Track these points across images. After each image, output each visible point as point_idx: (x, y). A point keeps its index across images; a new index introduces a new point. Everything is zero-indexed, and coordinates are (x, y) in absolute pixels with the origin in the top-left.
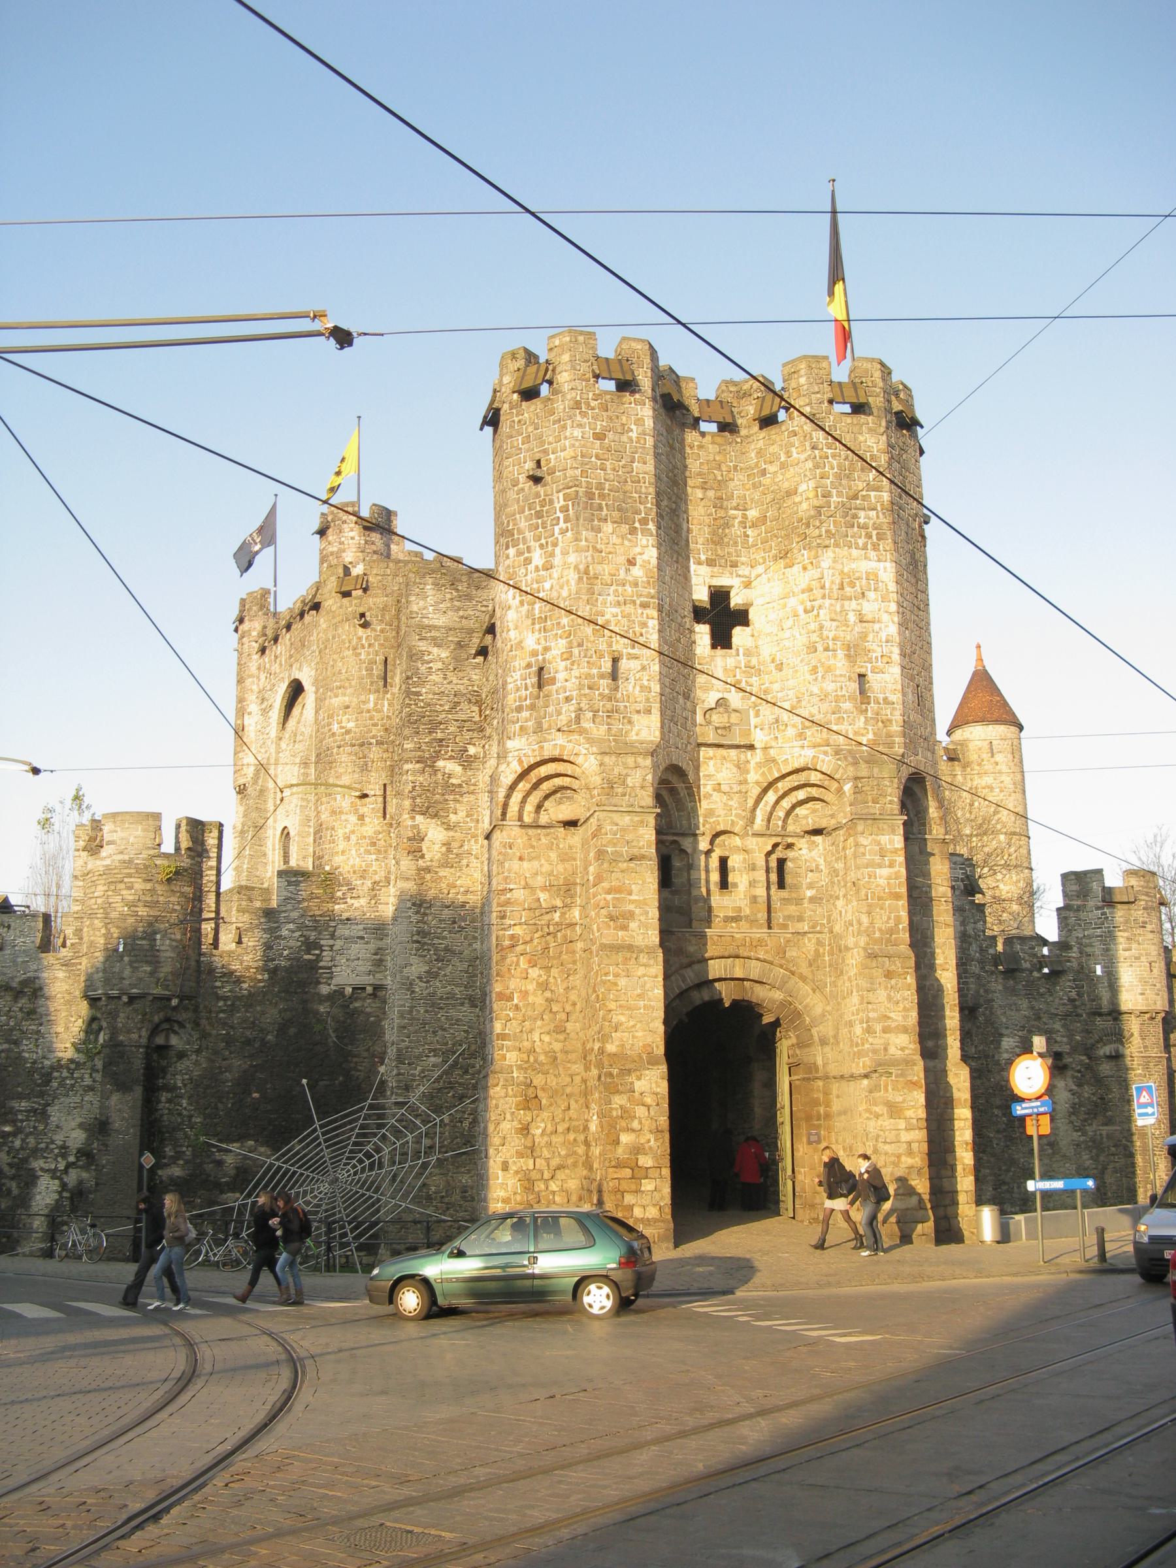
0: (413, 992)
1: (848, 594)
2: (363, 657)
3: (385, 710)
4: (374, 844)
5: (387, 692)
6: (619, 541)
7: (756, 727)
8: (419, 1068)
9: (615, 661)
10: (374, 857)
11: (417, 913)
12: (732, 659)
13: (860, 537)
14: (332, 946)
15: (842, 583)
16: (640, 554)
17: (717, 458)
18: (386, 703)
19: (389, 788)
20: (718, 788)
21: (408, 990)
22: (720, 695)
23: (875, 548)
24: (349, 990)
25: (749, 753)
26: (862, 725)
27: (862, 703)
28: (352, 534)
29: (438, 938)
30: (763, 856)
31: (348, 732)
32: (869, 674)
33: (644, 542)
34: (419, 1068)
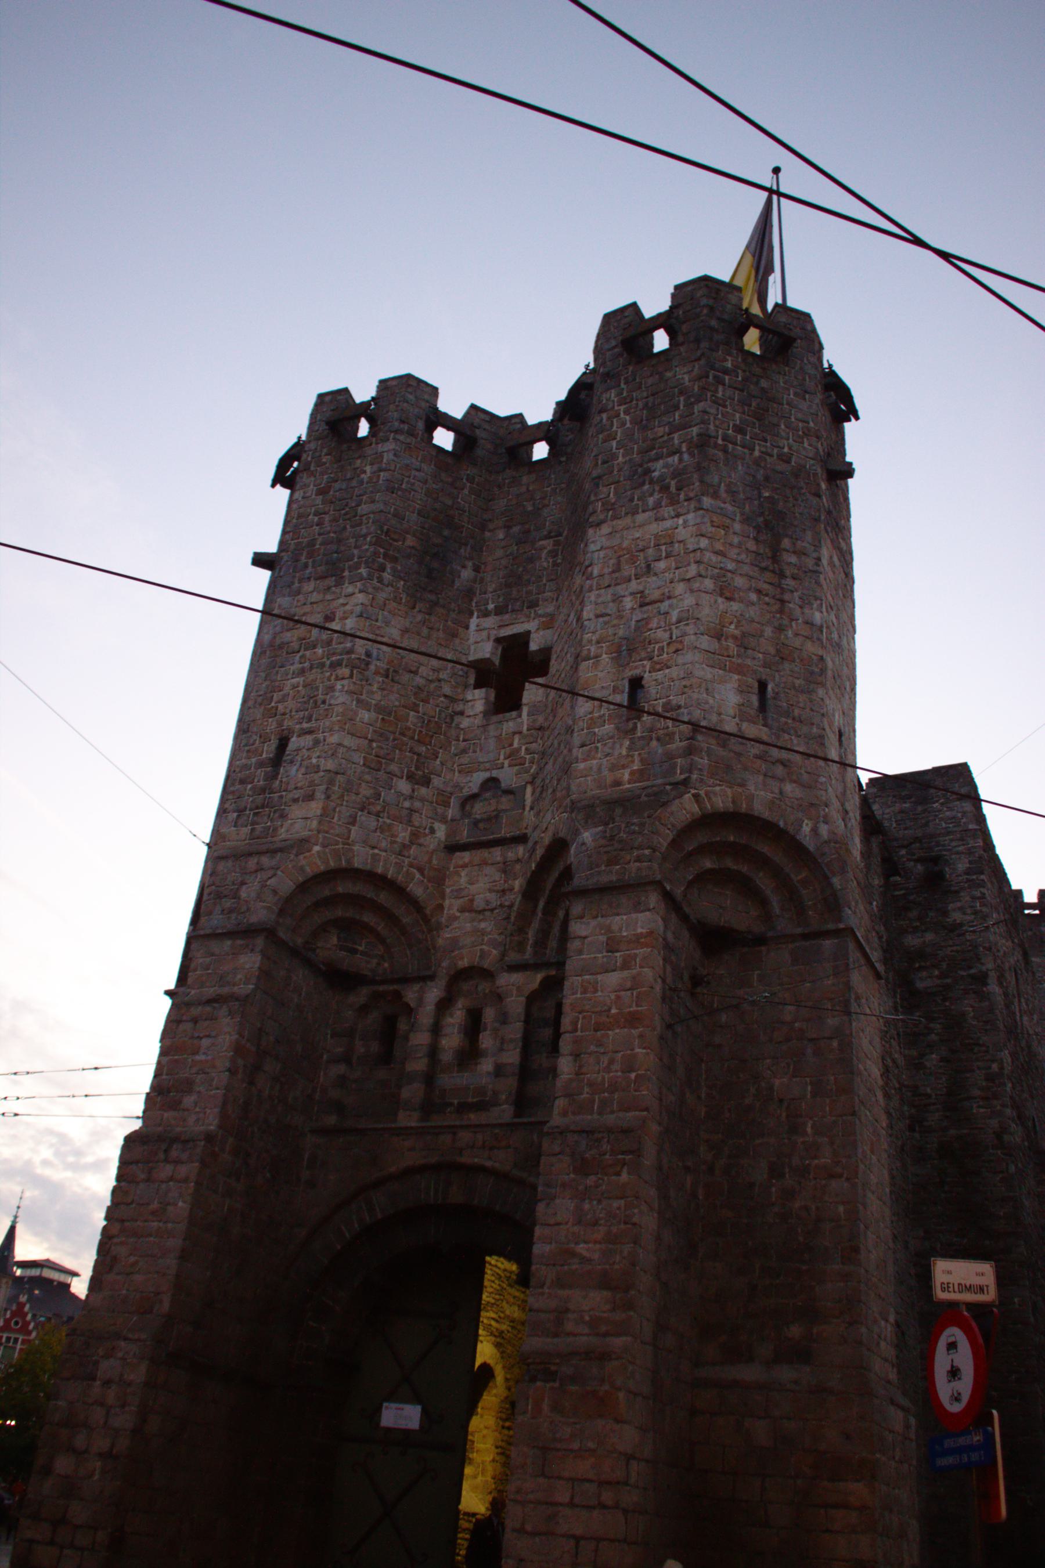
1: (626, 573)
6: (320, 597)
7: (532, 808)
9: (283, 743)
12: (511, 724)
13: (651, 495)
15: (619, 564)
16: (344, 605)
17: (531, 488)
20: (468, 908)
22: (487, 775)
23: (673, 502)
25: (521, 850)
26: (624, 752)
27: (628, 720)
30: (523, 999)
32: (646, 675)
33: (350, 589)
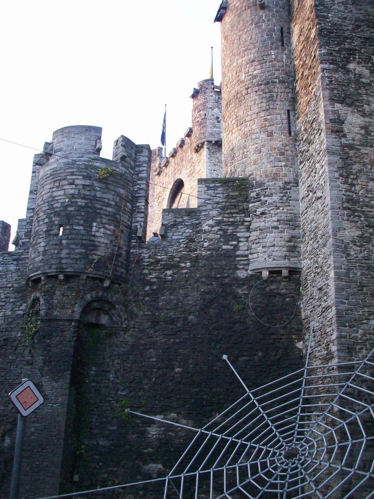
0: (348, 255)
2: (263, 27)
3: (284, 60)
4: (282, 154)
5: (283, 50)
8: (360, 331)
10: (283, 164)
11: (345, 183)
14: (248, 238)
18: (284, 56)
19: (291, 113)
21: (344, 252)
24: (265, 274)
28: (211, 94)
29: (366, 206)
31: (255, 77)
34: (360, 331)
